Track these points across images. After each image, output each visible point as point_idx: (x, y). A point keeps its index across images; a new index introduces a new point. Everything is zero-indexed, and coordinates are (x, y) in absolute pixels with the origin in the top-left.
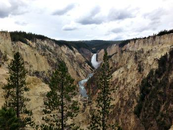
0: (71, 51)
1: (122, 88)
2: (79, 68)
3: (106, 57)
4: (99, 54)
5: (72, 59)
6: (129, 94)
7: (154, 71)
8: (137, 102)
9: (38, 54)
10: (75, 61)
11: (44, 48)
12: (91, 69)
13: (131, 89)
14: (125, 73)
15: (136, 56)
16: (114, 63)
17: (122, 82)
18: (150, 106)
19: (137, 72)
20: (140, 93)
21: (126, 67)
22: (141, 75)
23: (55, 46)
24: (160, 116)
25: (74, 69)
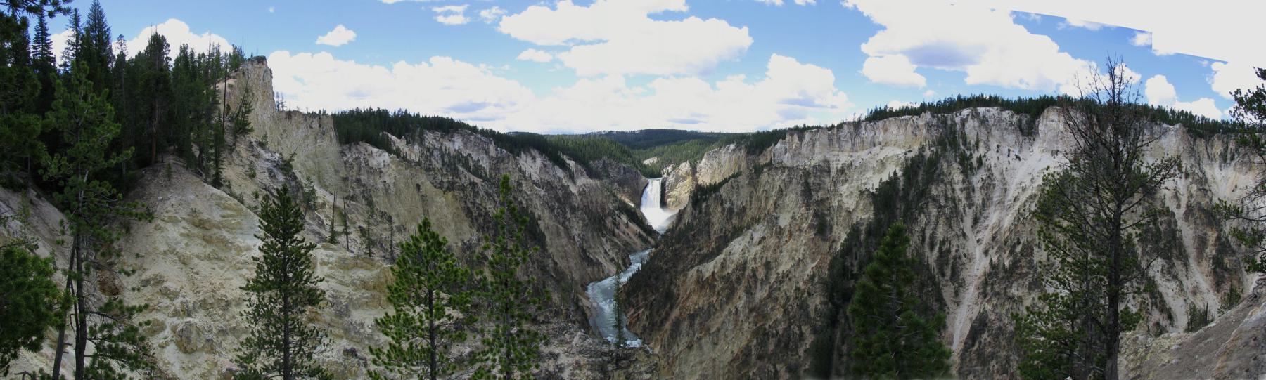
0: (560, 173)
1: (760, 294)
5: (561, 201)
6: (786, 312)
7: (863, 228)
8: (815, 331)
9: (427, 186)
10: (573, 209)
11: (453, 162)
13: (792, 293)
14: (772, 241)
15: (806, 184)
16: (731, 210)
17: (761, 273)
19: (812, 234)
21: (772, 221)
25: (571, 238)
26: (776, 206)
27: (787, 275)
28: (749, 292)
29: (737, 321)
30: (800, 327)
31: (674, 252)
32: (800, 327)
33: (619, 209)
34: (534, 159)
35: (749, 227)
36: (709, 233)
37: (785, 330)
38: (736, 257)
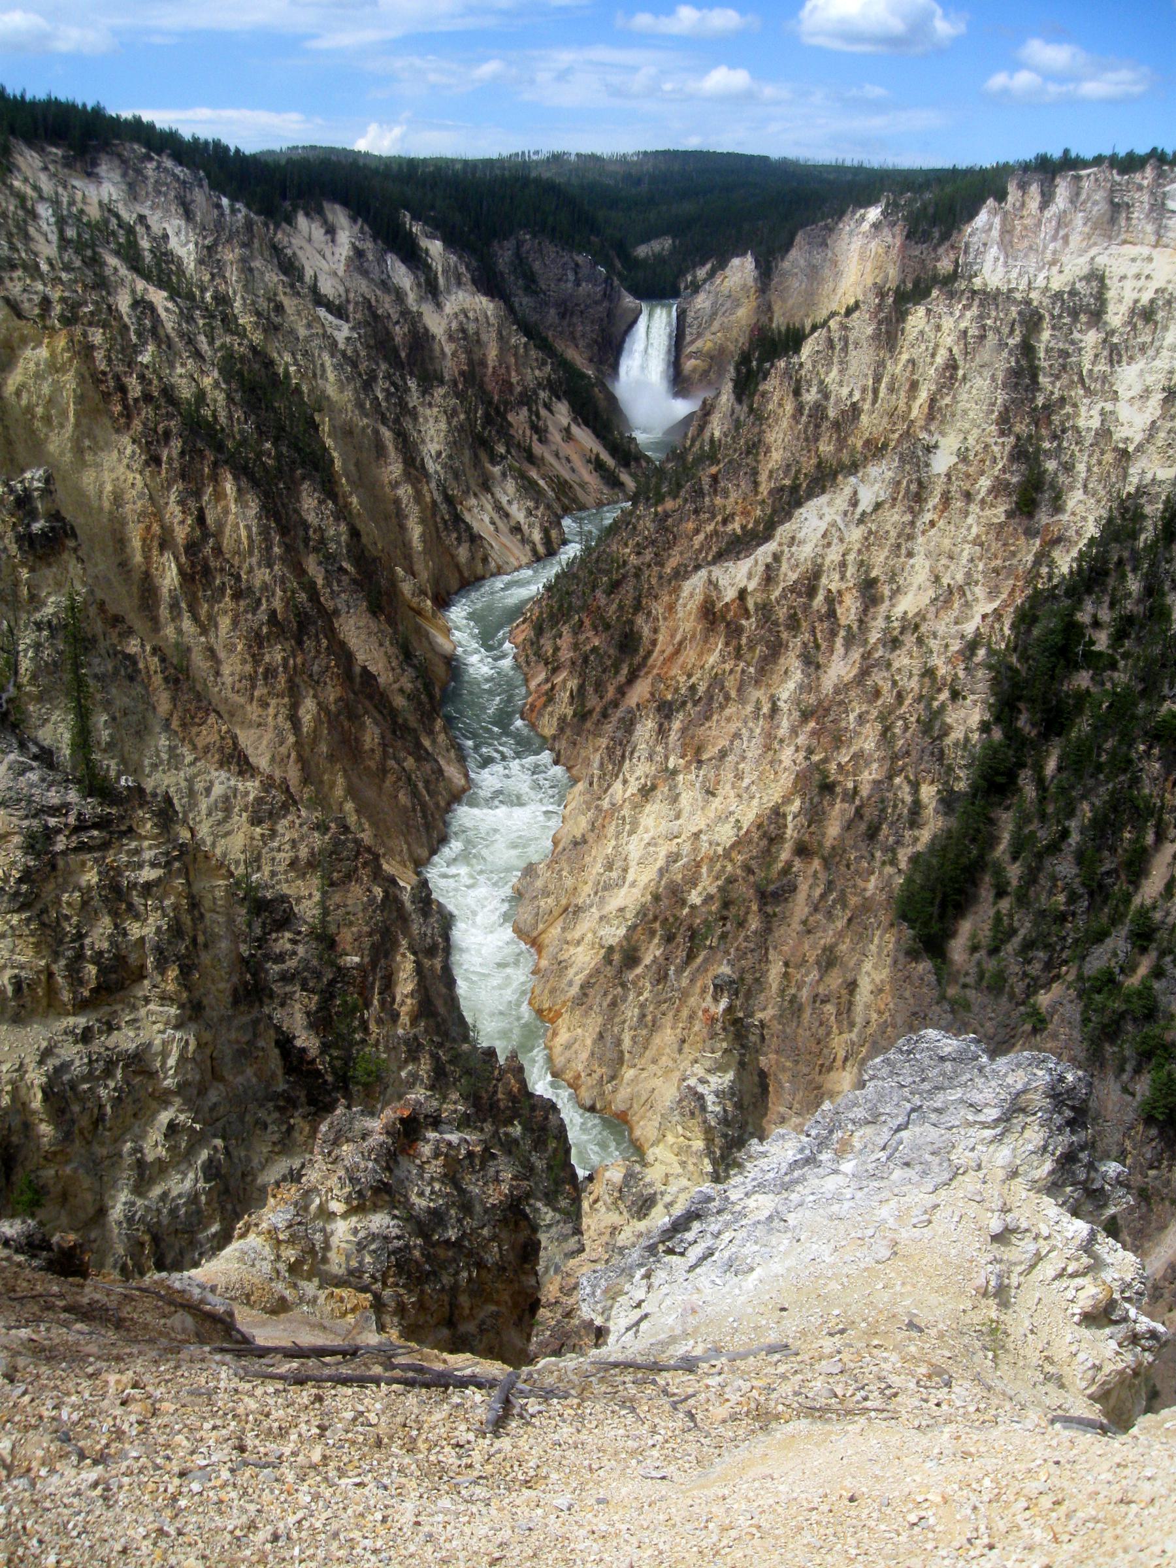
0: (402, 276)
1: (840, 668)
4: (702, 302)
7: (1153, 510)
12: (599, 465)
14: (894, 517)
15: (1027, 349)
16: (818, 412)
17: (849, 610)
18: (1054, 848)
19: (998, 513)
20: (985, 727)
24: (1118, 942)
26: (933, 410)
27: (912, 625)
28: (812, 662)
29: (769, 736)
31: (661, 520)
32: (915, 786)
34: (331, 231)
36: (755, 473)
37: (877, 783)
38: (806, 552)
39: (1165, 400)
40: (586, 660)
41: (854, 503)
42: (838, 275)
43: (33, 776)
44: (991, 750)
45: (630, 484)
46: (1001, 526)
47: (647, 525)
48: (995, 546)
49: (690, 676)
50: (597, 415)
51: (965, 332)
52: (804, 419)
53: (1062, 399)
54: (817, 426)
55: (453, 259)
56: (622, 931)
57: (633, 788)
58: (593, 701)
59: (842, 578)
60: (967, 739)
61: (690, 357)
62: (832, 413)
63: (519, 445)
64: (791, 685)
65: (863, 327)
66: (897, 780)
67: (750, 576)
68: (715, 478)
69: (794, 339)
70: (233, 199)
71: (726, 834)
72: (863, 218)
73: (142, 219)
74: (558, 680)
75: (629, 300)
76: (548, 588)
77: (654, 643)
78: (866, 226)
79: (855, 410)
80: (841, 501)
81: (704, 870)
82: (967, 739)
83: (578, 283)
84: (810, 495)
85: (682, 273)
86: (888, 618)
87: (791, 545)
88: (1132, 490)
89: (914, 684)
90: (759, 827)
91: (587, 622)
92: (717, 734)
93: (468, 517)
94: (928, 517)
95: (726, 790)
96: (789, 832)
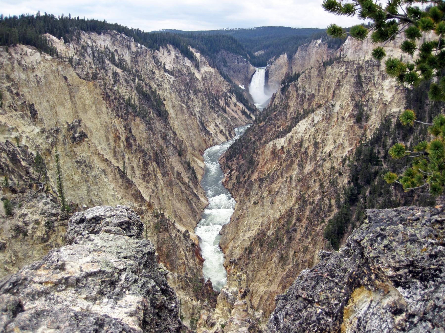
1: (309, 168)
2: (208, 110)
3: (289, 80)
5: (187, 85)
6: (321, 186)
7: (394, 120)
10: (196, 92)
12: (244, 113)
15: (359, 77)
16: (303, 96)
17: (311, 151)
19: (351, 122)
20: (349, 183)
21: (329, 108)
22: (359, 132)
23: (134, 49)
25: (192, 114)
26: (334, 95)
30: (330, 200)
32: (330, 200)
33: (230, 91)
34: (169, 52)
35: (313, 111)
36: (286, 114)
39: (396, 89)
40: (240, 167)
41: (313, 121)
42: (310, 58)
43: (49, 206)
44: (351, 190)
45: (254, 118)
46: (352, 126)
47: (257, 130)
48: (351, 132)
49: (268, 171)
50: (244, 99)
51: (342, 73)
52: (299, 98)
53: (368, 90)
54: (303, 100)
55: (203, 58)
56: (249, 243)
57: (252, 202)
58: (242, 179)
59: (309, 142)
60: (344, 186)
61: (271, 82)
62: (307, 97)
63: (222, 108)
64: (295, 173)
65: (315, 72)
66: (325, 198)
67: (285, 143)
68: (275, 115)
69: (297, 76)
70: (142, 44)
71: (278, 215)
72: (316, 43)
73: (116, 51)
74: (233, 173)
75: (252, 67)
76: (230, 148)
77: (259, 162)
78: (317, 45)
79: (313, 96)
80: (310, 121)
81: (271, 226)
82: (344, 186)
83: (238, 63)
84: (301, 119)
85: (267, 60)
86: (322, 153)
87: (296, 133)
88: (387, 114)
89: (329, 171)
90: (286, 213)
91: (240, 157)
92: (275, 187)
93: (208, 129)
94: (332, 124)
95: (278, 203)
96: (295, 214)
